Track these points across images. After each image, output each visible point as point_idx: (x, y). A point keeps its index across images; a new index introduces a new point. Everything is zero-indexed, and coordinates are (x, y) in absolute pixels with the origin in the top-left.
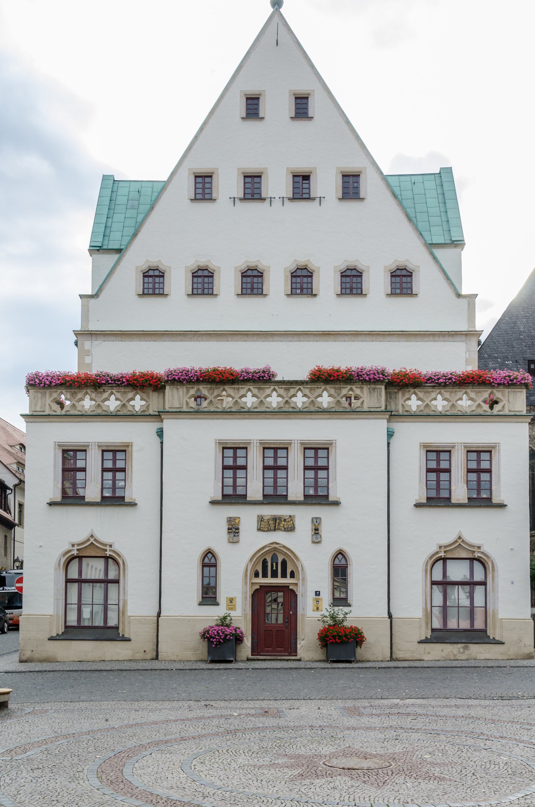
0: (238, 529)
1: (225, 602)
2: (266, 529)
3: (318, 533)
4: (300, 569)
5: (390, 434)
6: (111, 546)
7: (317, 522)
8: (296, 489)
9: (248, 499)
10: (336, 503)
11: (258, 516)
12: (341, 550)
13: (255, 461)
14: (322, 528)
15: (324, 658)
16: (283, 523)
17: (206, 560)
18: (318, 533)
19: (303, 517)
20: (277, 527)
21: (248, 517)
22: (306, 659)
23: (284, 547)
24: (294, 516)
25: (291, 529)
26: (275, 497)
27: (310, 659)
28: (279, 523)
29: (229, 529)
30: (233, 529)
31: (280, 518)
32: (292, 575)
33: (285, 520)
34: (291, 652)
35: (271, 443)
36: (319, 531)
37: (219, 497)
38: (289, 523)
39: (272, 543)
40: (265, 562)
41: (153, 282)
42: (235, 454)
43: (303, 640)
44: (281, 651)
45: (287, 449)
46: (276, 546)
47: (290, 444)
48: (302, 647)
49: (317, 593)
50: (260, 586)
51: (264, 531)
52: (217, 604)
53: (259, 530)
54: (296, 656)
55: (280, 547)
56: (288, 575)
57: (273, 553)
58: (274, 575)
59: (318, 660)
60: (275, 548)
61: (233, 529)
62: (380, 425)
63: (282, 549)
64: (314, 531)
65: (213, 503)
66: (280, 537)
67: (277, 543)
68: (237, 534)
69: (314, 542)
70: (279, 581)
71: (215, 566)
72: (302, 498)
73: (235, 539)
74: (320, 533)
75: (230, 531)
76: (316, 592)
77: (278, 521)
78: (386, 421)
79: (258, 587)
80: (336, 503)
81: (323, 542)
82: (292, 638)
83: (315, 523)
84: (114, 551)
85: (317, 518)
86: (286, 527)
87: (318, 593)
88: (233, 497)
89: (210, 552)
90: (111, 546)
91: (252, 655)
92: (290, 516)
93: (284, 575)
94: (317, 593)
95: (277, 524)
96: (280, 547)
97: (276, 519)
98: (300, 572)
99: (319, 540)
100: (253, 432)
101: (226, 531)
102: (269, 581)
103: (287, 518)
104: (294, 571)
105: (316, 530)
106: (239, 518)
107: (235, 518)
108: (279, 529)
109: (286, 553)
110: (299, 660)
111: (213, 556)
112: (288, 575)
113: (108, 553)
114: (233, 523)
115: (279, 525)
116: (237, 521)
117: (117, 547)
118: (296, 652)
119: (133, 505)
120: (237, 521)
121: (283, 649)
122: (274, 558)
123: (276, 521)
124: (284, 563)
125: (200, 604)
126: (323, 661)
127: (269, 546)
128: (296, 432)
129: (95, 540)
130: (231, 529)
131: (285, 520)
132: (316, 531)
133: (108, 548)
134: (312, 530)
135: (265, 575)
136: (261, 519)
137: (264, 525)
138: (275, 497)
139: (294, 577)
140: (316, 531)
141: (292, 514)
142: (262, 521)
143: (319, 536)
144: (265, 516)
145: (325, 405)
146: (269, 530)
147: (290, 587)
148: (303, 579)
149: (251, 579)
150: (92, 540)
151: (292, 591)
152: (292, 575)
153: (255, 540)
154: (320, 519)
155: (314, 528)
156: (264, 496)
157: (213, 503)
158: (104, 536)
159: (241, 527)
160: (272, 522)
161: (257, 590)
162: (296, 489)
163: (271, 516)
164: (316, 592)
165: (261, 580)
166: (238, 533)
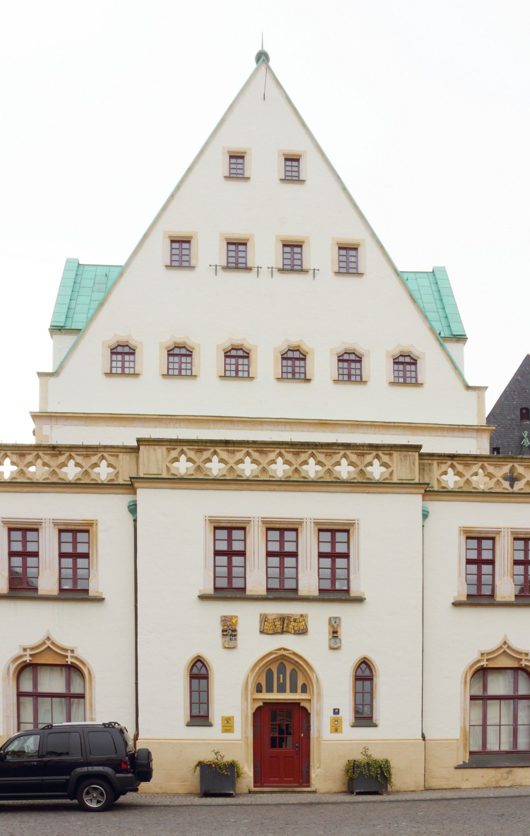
0: (235, 631)
1: (220, 722)
2: (271, 632)
3: (337, 637)
4: (314, 681)
5: (425, 515)
6: (72, 651)
7: (335, 622)
8: (309, 581)
9: (248, 593)
10: (360, 600)
11: (261, 615)
12: (365, 658)
13: (256, 544)
14: (342, 630)
15: (346, 790)
16: (293, 623)
17: (195, 671)
18: (337, 637)
19: (318, 616)
20: (285, 629)
21: (248, 616)
22: (322, 790)
23: (295, 654)
24: (306, 616)
25: (303, 632)
26: (282, 591)
27: (327, 790)
28: (288, 624)
29: (223, 631)
30: (229, 631)
31: (289, 617)
32: (304, 689)
33: (295, 621)
34: (302, 783)
35: (276, 522)
36: (339, 635)
37: (210, 590)
38: (300, 624)
39: (280, 649)
40: (269, 675)
41: (123, 353)
42: (230, 535)
43: (318, 768)
44: (290, 782)
45: (296, 530)
46: (284, 653)
47: (301, 523)
48: (317, 776)
49: (336, 712)
50: (264, 703)
51: (269, 634)
52: (210, 725)
53: (262, 632)
54: (309, 786)
55: (290, 653)
56: (299, 690)
57: (279, 662)
58: (282, 689)
59: (337, 791)
61: (229, 631)
62: (414, 502)
63: (292, 656)
64: (332, 634)
65: (203, 597)
66: (289, 642)
67: (285, 649)
68: (234, 638)
69: (332, 648)
70: (288, 696)
71: (206, 677)
72: (316, 593)
73: (232, 644)
74: (339, 637)
75: (225, 633)
76: (334, 710)
77: (286, 621)
78: (420, 497)
79: (261, 704)
80: (360, 600)
81: (342, 648)
82: (304, 766)
83: (333, 624)
84: (76, 658)
85: (336, 618)
86: (296, 628)
87: (337, 711)
88: (228, 590)
89: (199, 660)
90: (72, 651)
91: (255, 786)
92: (302, 616)
93: (294, 690)
94: (336, 712)
95: (285, 625)
96: (290, 653)
97: (283, 619)
98: (315, 686)
99: (339, 645)
100: (255, 507)
101: (220, 633)
102: (275, 696)
103: (297, 617)
104: (306, 683)
105: (335, 632)
106: (237, 617)
107: (231, 618)
108: (287, 632)
109: (297, 662)
110: (314, 792)
111: (204, 665)
112: (299, 690)
113: (70, 660)
114: (228, 623)
115: (287, 626)
116: (234, 621)
117: (80, 653)
119: (100, 600)
120: (234, 621)
121: (292, 779)
122: (282, 669)
123: (284, 621)
124: (294, 674)
125: (188, 725)
126: (344, 792)
127: (275, 653)
128: (310, 508)
129: (53, 643)
130: (226, 631)
131: (295, 621)
132: (335, 633)
133: (69, 654)
134: (329, 633)
135: (270, 690)
136: (264, 619)
137: (268, 626)
138: (282, 591)
140: (335, 633)
141: (303, 613)
142: (265, 621)
143: (338, 641)
144: (270, 615)
145: (344, 476)
146: (275, 633)
147: (302, 704)
148: (319, 694)
149: (252, 694)
150: (48, 644)
151: (305, 709)
152: (304, 689)
153: (256, 646)
154: (339, 619)
155: (332, 630)
156: (268, 590)
157: (203, 597)
158: (64, 639)
159: (238, 628)
160: (279, 623)
161: (259, 709)
162: (309, 581)
163: (277, 614)
164: (334, 710)
166: (235, 635)
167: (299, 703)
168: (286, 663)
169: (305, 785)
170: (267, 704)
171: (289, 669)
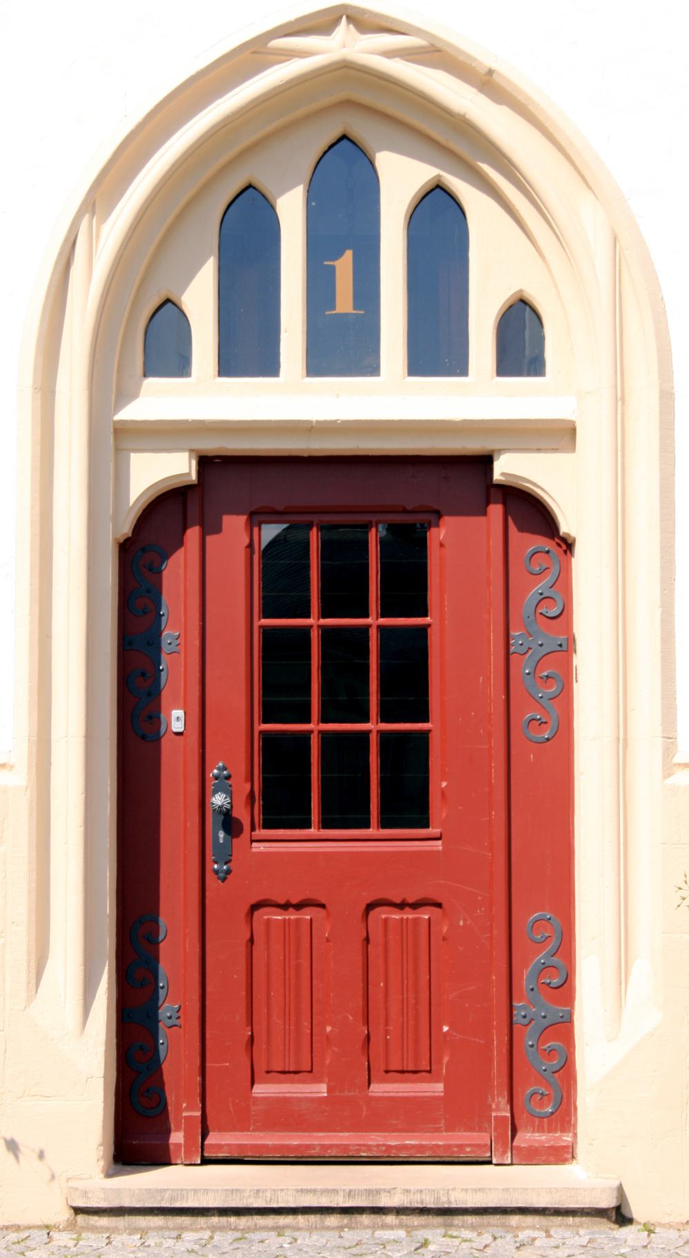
39: (321, 24)
50: (205, 462)
54: (562, 1155)
58: (342, 346)
60: (346, 70)
67: (364, 23)
70: (388, 401)
79: (177, 466)
93: (437, 350)
102: (296, 401)
118: (563, 1114)
122: (343, 184)
124: (438, 217)
135: (247, 350)
139: (535, 366)
147: (505, 468)
149: (107, 388)
165: (208, 399)
167: (485, 461)
168: (362, 130)
169: (540, 1138)
170: (230, 476)
171: (400, 178)
